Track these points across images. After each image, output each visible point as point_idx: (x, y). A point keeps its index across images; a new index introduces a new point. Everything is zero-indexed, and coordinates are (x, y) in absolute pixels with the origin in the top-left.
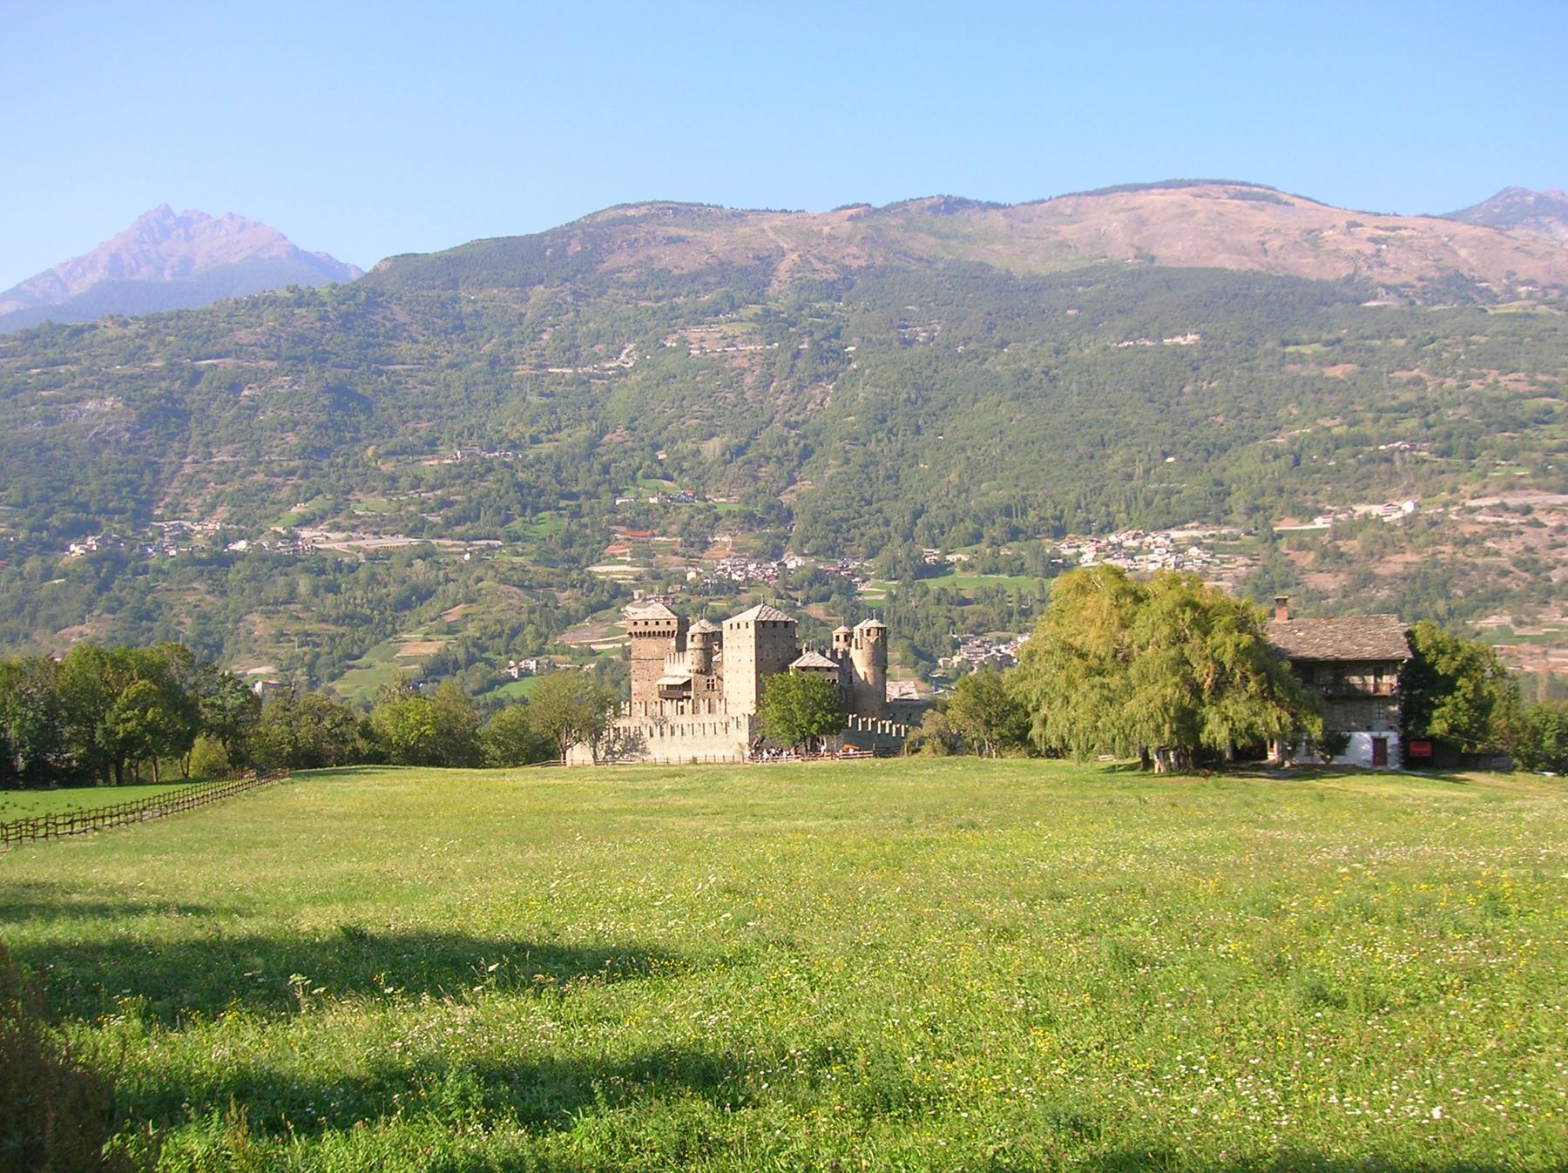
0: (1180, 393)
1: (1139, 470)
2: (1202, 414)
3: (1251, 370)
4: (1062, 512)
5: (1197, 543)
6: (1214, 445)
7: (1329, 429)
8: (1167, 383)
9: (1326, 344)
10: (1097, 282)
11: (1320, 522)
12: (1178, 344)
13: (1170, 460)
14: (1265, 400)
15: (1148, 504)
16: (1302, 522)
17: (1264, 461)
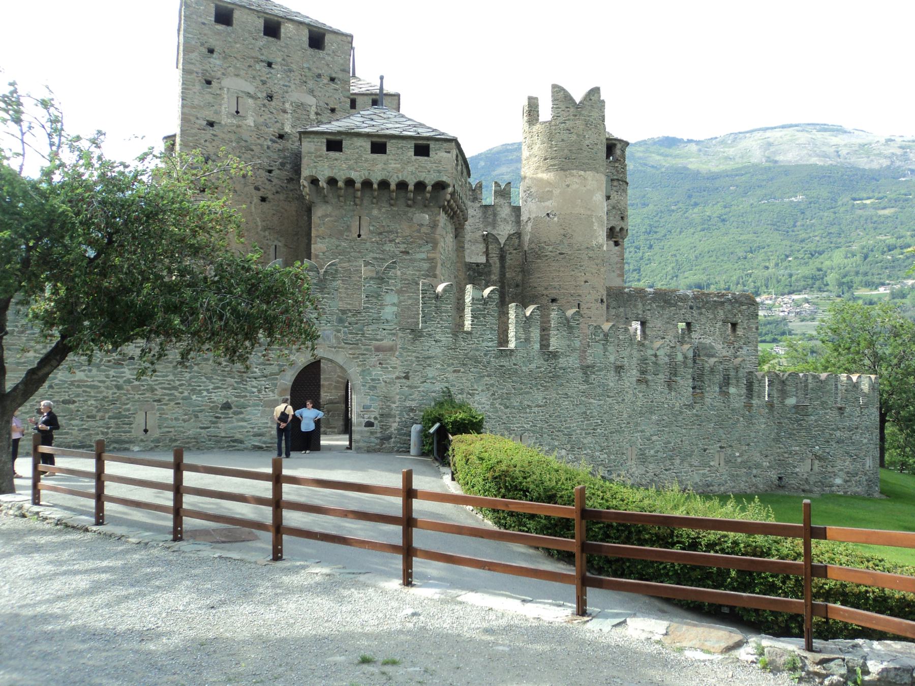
0: (795, 226)
1: (772, 264)
2: (807, 236)
3: (835, 213)
4: (729, 286)
5: (807, 301)
6: (815, 252)
7: (884, 241)
8: (787, 221)
9: (877, 199)
10: (746, 173)
11: (882, 290)
12: (792, 201)
13: (790, 259)
14: (843, 228)
15: (778, 282)
16: (871, 290)
17: (846, 257)
